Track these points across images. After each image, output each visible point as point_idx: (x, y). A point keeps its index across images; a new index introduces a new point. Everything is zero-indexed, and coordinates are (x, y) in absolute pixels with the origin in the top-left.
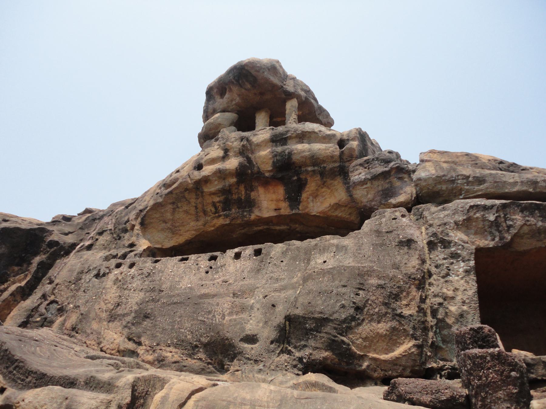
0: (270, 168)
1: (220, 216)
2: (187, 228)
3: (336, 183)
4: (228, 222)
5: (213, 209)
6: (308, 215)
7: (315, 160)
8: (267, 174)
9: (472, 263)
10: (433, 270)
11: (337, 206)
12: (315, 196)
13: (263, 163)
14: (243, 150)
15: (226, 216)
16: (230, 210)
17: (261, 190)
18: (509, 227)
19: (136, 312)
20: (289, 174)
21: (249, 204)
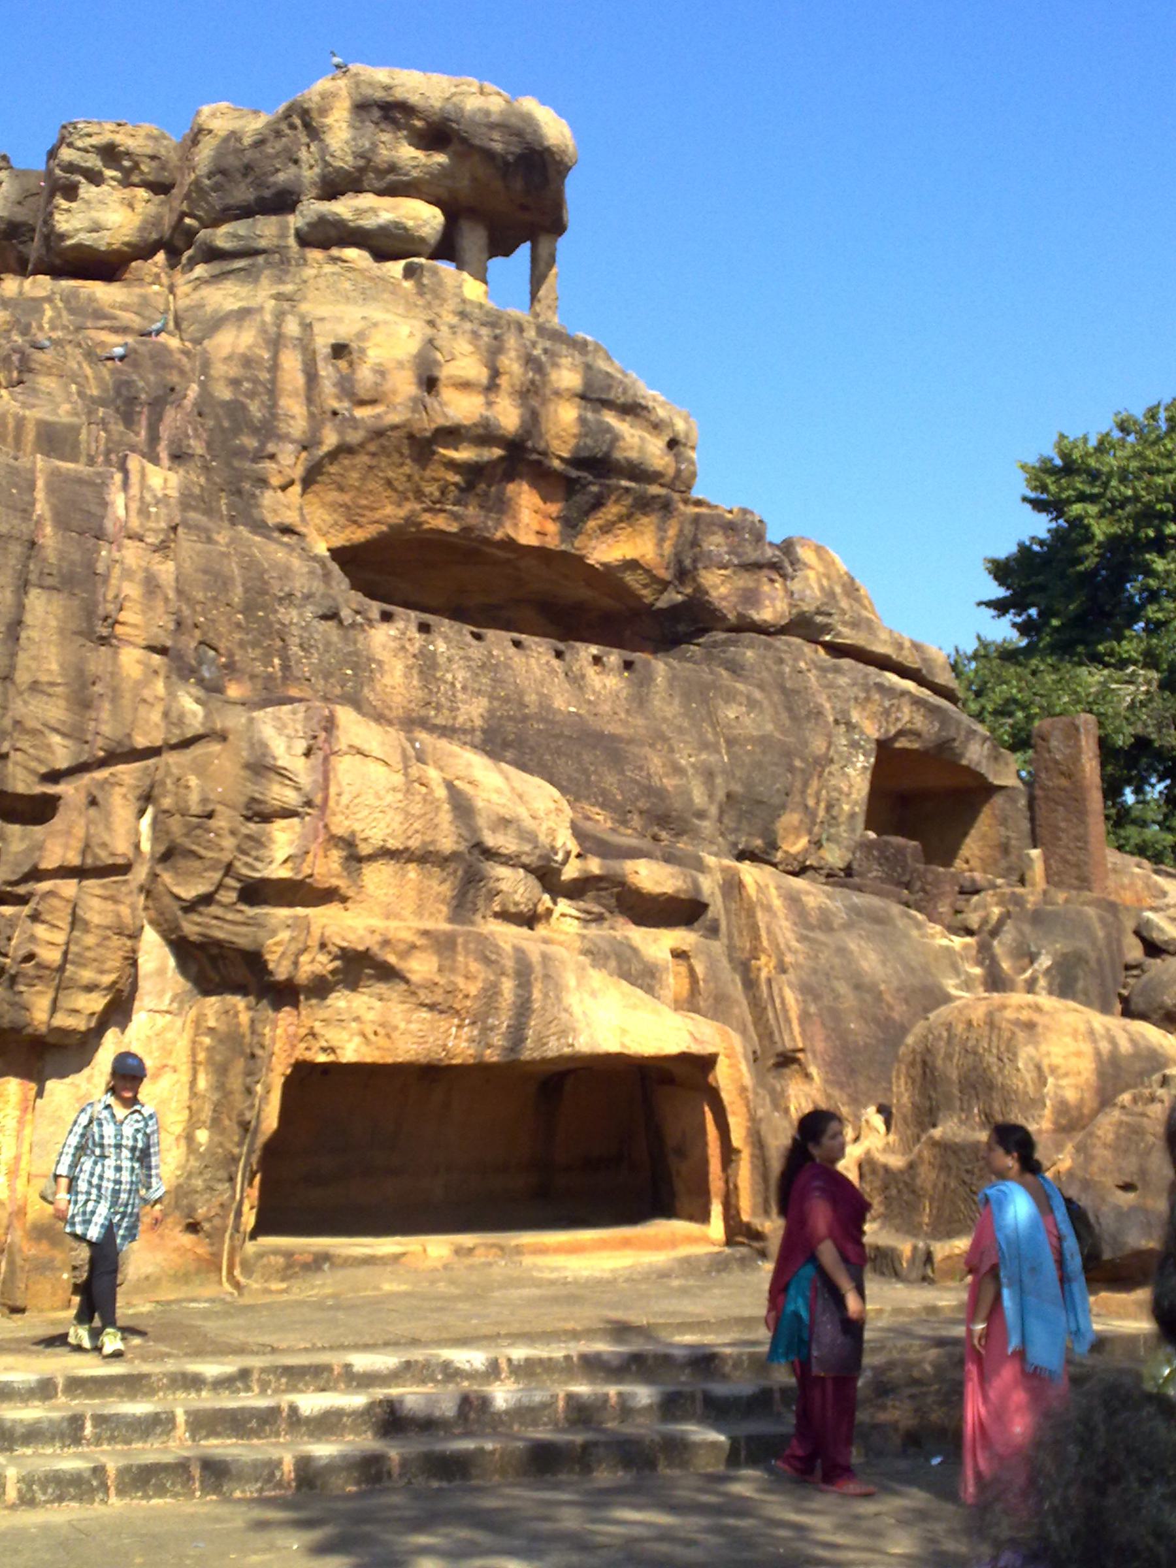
0: (565, 455)
1: (442, 511)
2: (377, 515)
3: (645, 520)
4: (454, 528)
5: (437, 494)
6: (581, 559)
7: (639, 472)
8: (556, 463)
9: (872, 760)
10: (836, 757)
11: (632, 565)
12: (606, 529)
13: (559, 437)
14: (528, 391)
15: (456, 517)
16: (466, 506)
17: (525, 487)
18: (898, 719)
19: (484, 731)
20: (591, 479)
21: (502, 507)
